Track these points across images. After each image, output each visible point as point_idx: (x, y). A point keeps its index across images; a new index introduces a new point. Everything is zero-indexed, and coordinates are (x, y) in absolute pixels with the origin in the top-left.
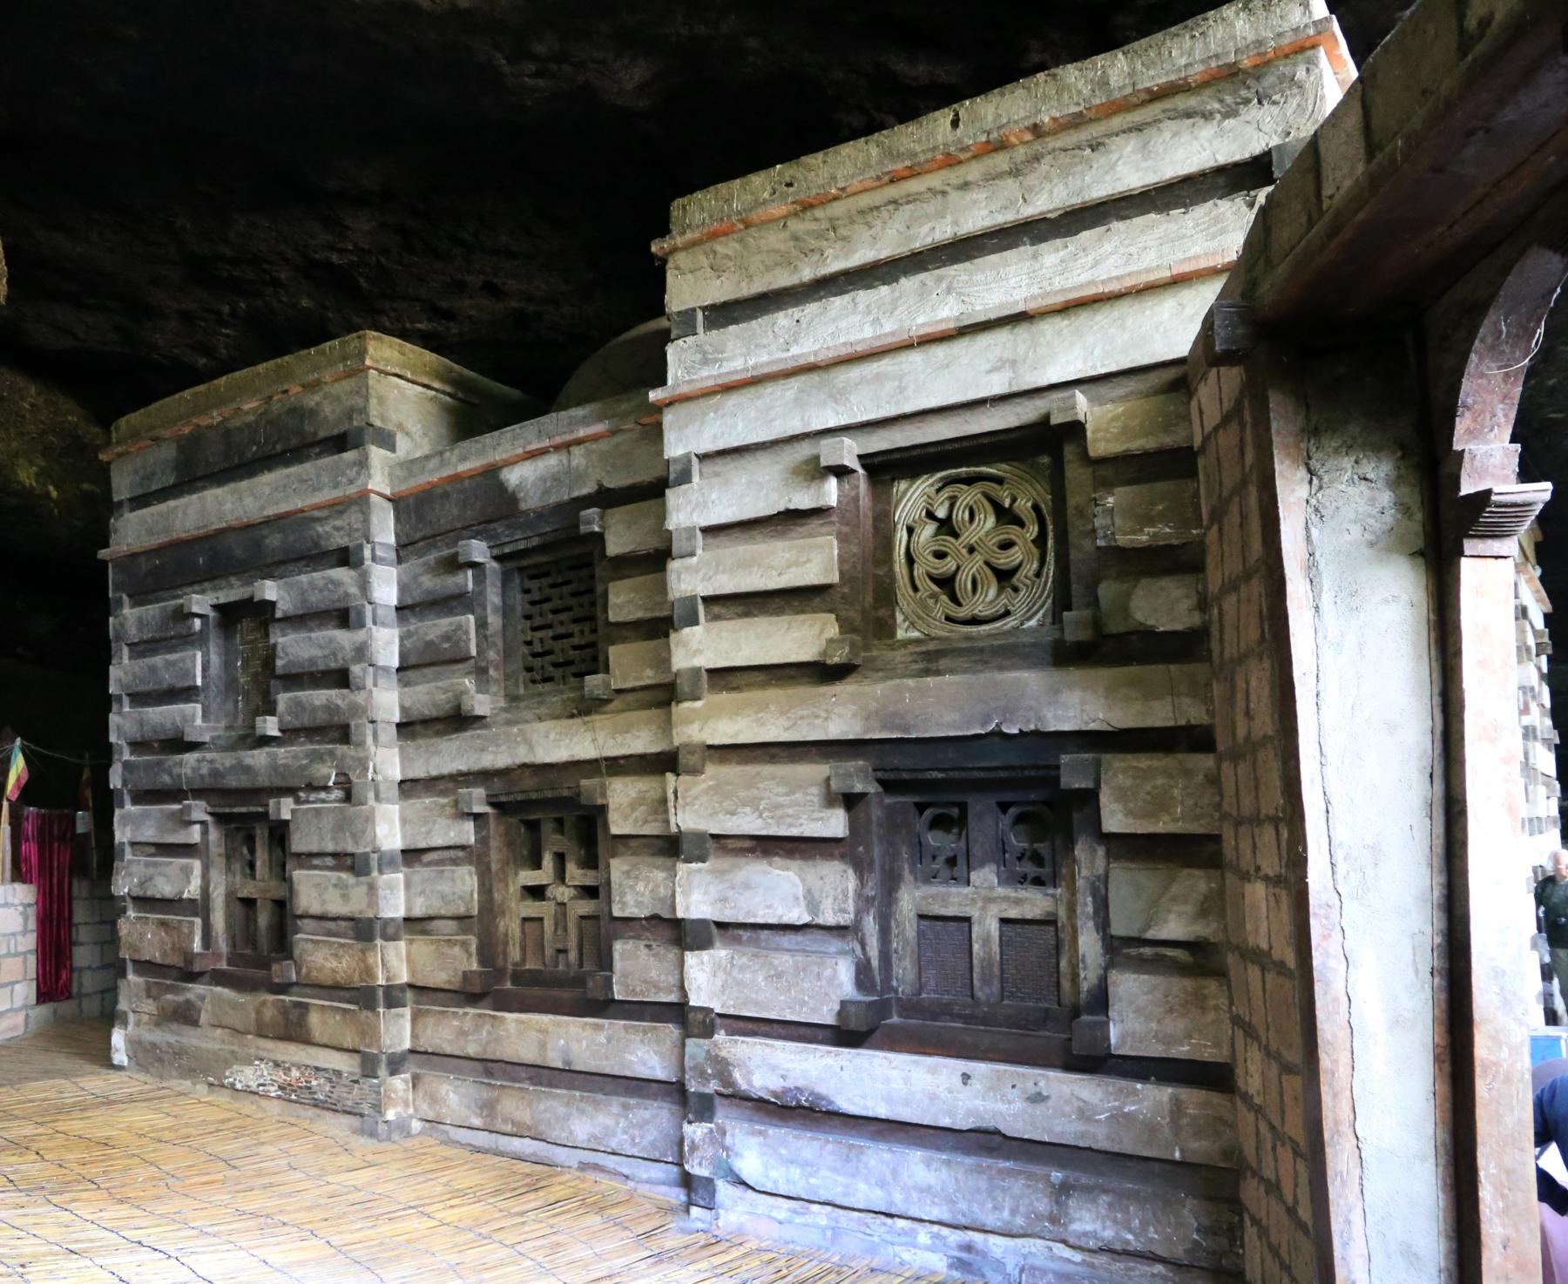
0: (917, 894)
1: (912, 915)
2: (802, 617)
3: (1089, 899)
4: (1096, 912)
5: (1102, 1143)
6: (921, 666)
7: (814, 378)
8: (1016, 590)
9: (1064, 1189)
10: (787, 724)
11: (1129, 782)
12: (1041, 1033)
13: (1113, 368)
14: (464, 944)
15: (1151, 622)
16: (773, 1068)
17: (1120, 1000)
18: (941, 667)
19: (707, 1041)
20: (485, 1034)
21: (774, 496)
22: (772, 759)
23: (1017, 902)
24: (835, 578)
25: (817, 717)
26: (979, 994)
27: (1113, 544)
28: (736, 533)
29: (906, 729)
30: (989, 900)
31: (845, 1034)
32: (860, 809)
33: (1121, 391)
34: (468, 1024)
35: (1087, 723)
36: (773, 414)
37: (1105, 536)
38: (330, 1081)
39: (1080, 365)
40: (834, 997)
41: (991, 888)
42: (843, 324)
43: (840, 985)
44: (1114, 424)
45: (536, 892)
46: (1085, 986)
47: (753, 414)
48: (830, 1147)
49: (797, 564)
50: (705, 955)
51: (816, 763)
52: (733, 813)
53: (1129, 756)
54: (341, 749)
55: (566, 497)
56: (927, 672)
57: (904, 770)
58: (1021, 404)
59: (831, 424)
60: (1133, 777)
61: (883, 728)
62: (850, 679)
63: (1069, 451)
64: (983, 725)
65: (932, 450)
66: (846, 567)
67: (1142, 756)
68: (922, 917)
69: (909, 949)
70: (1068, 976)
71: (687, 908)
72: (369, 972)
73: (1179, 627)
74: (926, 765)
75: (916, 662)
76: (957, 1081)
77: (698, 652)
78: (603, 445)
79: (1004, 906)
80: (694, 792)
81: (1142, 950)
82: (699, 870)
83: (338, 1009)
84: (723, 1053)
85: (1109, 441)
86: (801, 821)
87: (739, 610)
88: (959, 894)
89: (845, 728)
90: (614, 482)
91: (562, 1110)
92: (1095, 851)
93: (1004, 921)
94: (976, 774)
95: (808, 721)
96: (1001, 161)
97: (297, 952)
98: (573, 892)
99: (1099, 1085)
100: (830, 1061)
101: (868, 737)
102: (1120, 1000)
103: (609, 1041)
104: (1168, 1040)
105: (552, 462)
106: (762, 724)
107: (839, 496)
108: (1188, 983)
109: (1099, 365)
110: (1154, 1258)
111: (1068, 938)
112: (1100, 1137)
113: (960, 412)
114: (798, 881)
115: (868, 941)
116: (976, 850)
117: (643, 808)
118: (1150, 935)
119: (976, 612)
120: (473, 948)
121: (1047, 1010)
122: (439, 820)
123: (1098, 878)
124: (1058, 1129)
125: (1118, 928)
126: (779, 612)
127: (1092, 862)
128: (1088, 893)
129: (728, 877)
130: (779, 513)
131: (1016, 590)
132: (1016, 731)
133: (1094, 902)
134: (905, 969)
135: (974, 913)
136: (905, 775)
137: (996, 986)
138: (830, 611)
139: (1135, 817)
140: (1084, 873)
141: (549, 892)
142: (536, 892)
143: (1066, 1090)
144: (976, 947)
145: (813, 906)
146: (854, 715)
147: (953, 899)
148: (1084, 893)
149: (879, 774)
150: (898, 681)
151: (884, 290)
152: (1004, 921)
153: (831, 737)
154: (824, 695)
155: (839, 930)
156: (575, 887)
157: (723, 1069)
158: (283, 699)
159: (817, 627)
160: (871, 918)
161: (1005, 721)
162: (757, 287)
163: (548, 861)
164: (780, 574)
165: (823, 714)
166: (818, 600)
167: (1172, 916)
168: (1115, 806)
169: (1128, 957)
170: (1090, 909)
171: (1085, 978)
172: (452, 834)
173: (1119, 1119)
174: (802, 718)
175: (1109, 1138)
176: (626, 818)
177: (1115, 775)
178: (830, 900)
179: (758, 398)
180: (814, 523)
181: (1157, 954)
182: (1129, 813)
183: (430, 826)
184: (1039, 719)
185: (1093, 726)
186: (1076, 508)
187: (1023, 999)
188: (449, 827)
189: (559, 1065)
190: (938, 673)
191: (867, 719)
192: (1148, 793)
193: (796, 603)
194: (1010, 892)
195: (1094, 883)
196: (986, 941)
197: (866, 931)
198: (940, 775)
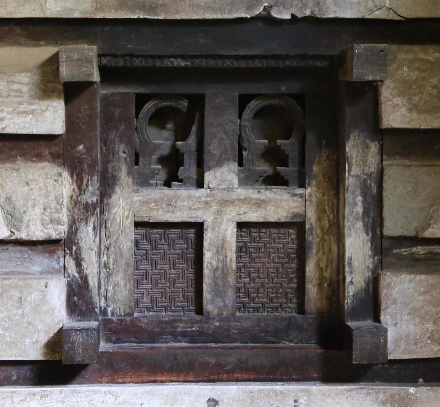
1: (129, 223)
3: (360, 198)
4: (366, 212)
11: (414, 75)
12: (281, 345)
17: (394, 302)
23: (259, 204)
29: (152, 9)
30: (224, 203)
35: (372, 11)
40: (40, 327)
41: (230, 190)
43: (51, 312)
51: (20, 44)
53: (416, 48)
57: (137, 56)
60: (418, 69)
61: (121, 6)
64: (249, 8)
67: (430, 49)
68: (138, 225)
69: (122, 262)
70: (315, 282)
74: (169, 51)
79: (244, 209)
81: (414, 249)
88: (189, 197)
92: (368, 147)
93: (241, 225)
94: (228, 63)
99: (368, 394)
101: (100, 16)
102: (394, 302)
111: (317, 240)
115: (85, 255)
118: (428, 234)
121: (290, 318)
123: (370, 175)
127: (364, 161)
128: (358, 192)
132: (288, 17)
133: (364, 201)
134: (116, 285)
136: (137, 62)
137: (231, 295)
139: (419, 112)
140: (355, 170)
144: (208, 256)
148: (354, 192)
149: (105, 61)
152: (241, 225)
153: (48, 15)
160: (91, 229)
161: (276, 4)
168: (398, 100)
169: (399, 257)
170: (360, 209)
171: (351, 282)
177: (399, 67)
178: (38, 210)
181: (431, 253)
185: (377, 14)
187: (257, 309)
192: (435, 87)
197: (83, 245)
198: (183, 64)
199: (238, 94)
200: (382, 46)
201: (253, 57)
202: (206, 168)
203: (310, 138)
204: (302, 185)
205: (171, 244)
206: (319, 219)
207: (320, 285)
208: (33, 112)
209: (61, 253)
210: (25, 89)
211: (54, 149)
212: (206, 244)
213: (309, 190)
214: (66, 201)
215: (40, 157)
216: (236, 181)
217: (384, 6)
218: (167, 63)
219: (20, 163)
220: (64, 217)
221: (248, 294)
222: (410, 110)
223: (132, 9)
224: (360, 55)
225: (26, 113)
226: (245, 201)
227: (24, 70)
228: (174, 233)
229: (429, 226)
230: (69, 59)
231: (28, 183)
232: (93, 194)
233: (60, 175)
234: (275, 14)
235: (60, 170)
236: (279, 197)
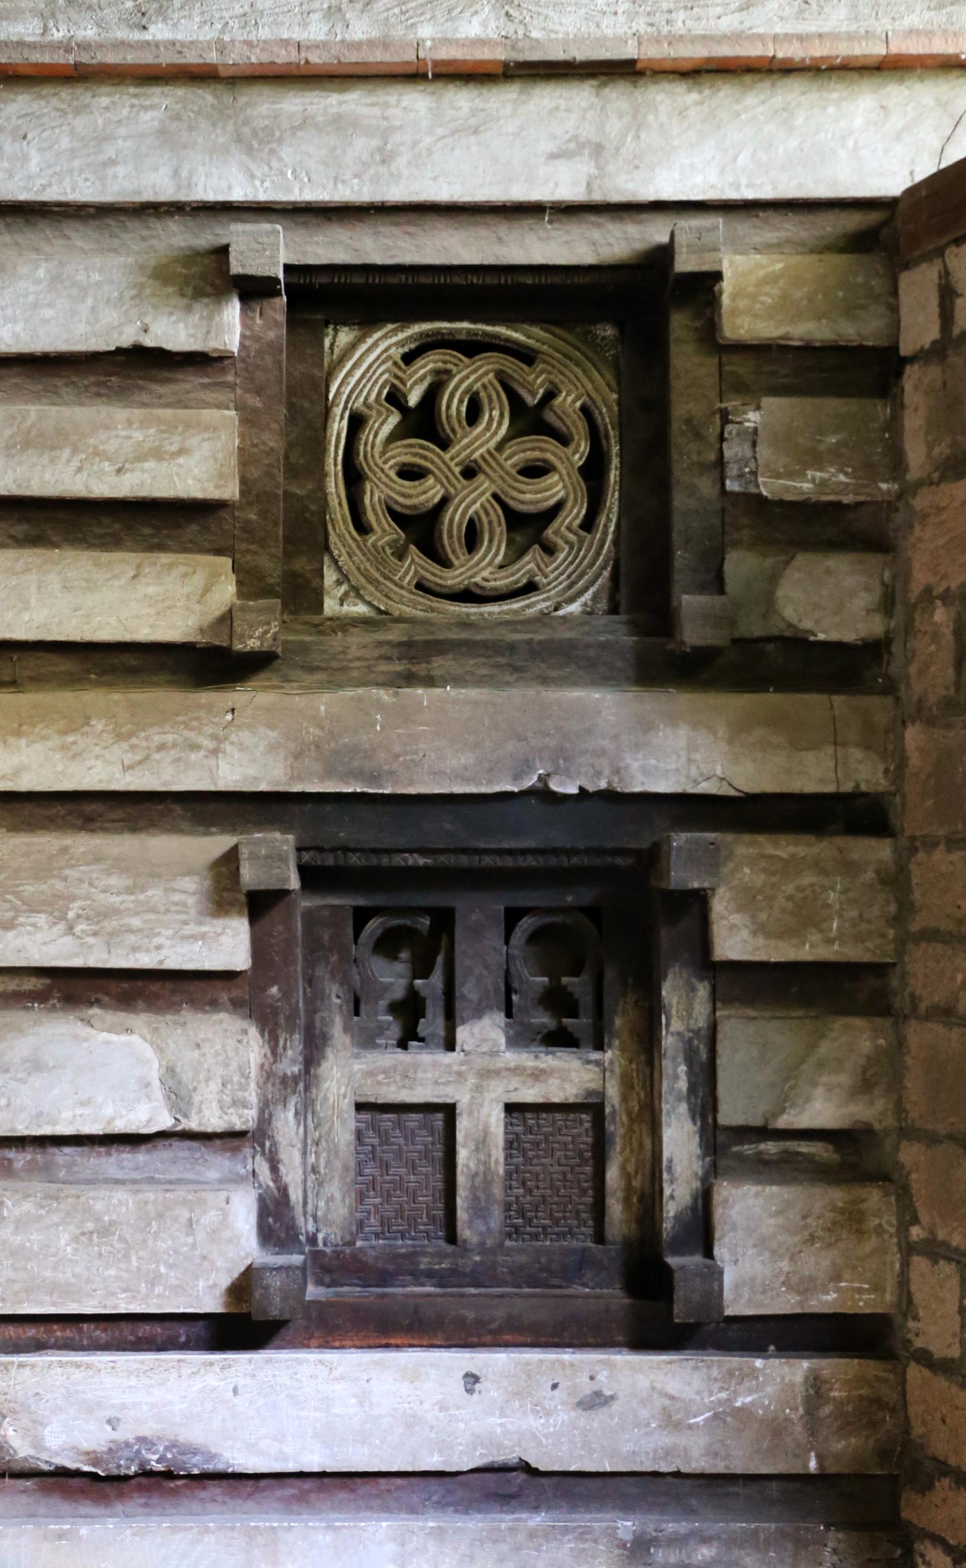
0: (357, 1066)
1: (347, 1105)
2: (165, 558)
5: (698, 1463)
6: (398, 667)
7: (205, 97)
8: (550, 550)
10: (128, 758)
11: (760, 880)
12: (570, 1291)
13: (766, 193)
15: (807, 624)
16: (90, 1409)
18: (436, 673)
21: (110, 316)
22: (88, 824)
23: (538, 1075)
24: (230, 491)
25: (195, 747)
26: (465, 1232)
27: (753, 490)
29: (374, 778)
30: (487, 1074)
32: (274, 920)
33: (770, 236)
35: (696, 783)
36: (110, 151)
37: (741, 476)
39: (713, 178)
41: (494, 1054)
44: (767, 289)
46: (671, 1210)
47: (65, 142)
49: (157, 454)
51: (181, 832)
53: (761, 838)
56: (410, 679)
57: (354, 850)
58: (599, 226)
59: (238, 194)
60: (764, 870)
61: (329, 773)
62: (257, 681)
64: (517, 777)
65: (426, 280)
66: (255, 473)
67: (783, 839)
68: (361, 1107)
69: (338, 1165)
70: (620, 1194)
73: (849, 636)
74: (402, 842)
75: (388, 658)
76: (456, 1385)
79: (515, 1082)
85: (756, 316)
86: (157, 941)
87: (20, 529)
88: (435, 1065)
89: (252, 771)
92: (693, 989)
93: (511, 1109)
94: (487, 860)
95: (174, 753)
100: (211, 1379)
101: (297, 788)
104: (805, 1287)
107: (243, 336)
108: (838, 1195)
109: (744, 181)
111: (622, 1131)
112: (696, 1452)
113: (489, 218)
116: (467, 990)
119: (478, 579)
121: (584, 1250)
123: (697, 1032)
124: (626, 1448)
126: (112, 542)
127: (689, 1009)
130: (119, 351)
131: (550, 550)
132: (573, 790)
135: (461, 1096)
136: (355, 860)
138: (219, 552)
139: (768, 936)
140: (677, 1025)
143: (643, 1382)
144: (462, 1155)
146: (272, 748)
149: (306, 857)
150: (360, 691)
152: (511, 1109)
153: (222, 786)
154: (209, 708)
159: (198, 580)
161: (556, 772)
164: (119, 471)
165: (208, 744)
166: (194, 528)
167: (819, 1091)
174: (161, 748)
175: (712, 1453)
177: (738, 869)
179: (78, 111)
180: (190, 382)
182: (759, 929)
184: (617, 771)
185: (705, 787)
186: (689, 421)
187: (535, 1237)
190: (430, 681)
191: (297, 756)
192: (790, 898)
193: (147, 531)
194: (525, 1059)
195: (690, 1040)
196: (482, 1142)
198: (422, 861)
199: (502, 908)
200: (711, 836)
201: (524, 852)
202: (458, 1020)
203: (610, 975)
204: (599, 1046)
205: (410, 1136)
206: (624, 1099)
207: (627, 1200)
208: (203, 937)
209: (248, 1151)
210: (191, 901)
211: (236, 993)
212: (460, 1137)
213: (609, 1054)
214: (254, 1072)
216: (503, 1040)
217: (715, 775)
218: (398, 860)
219: (187, 1014)
220: (252, 1095)
221: (522, 1213)
222: (754, 933)
223: (345, 777)
224: (679, 848)
225: (194, 937)
226: (517, 1071)
227: (189, 872)
228: (413, 1120)
229: (783, 1111)
230: (254, 857)
231: (198, 1046)
232: (294, 1061)
233: (245, 1032)
234: (556, 786)
235: (245, 1024)
236: (566, 1066)
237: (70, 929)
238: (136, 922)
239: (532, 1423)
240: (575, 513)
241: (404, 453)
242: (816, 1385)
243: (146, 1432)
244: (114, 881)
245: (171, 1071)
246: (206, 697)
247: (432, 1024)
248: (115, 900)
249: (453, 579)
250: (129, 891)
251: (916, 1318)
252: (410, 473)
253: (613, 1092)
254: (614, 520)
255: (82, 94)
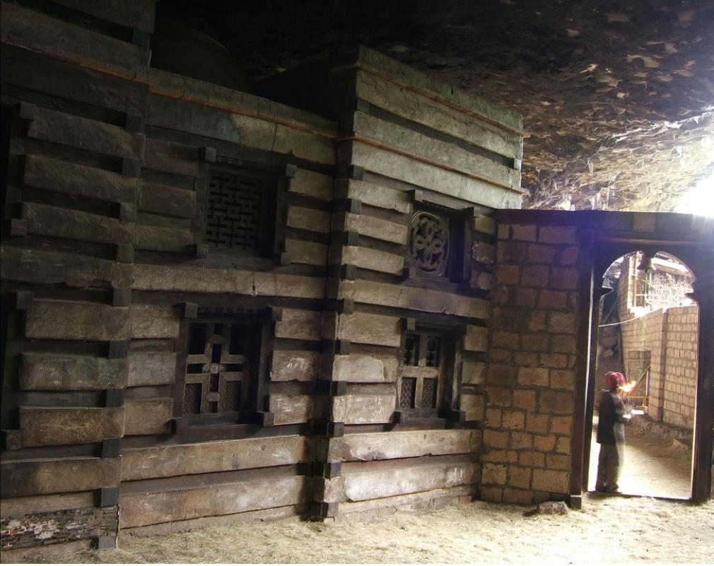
7: (408, 160)
9: (446, 470)
14: (165, 403)
19: (340, 438)
20: (177, 460)
21: (390, 202)
23: (429, 372)
26: (416, 406)
28: (371, 210)
31: (394, 423)
34: (164, 455)
38: (57, 520)
42: (417, 144)
45: (197, 369)
48: (383, 474)
50: (343, 398)
52: (362, 333)
54: (103, 262)
55: (269, 149)
63: (467, 223)
71: (337, 377)
72: (115, 429)
77: (355, 258)
78: (296, 132)
80: (347, 322)
82: (345, 359)
83: (75, 462)
84: (347, 442)
90: (299, 154)
91: (232, 494)
96: (463, 117)
97: (24, 422)
98: (221, 367)
103: (263, 449)
105: (266, 125)
106: (377, 296)
110: (459, 486)
114: (382, 364)
116: (421, 354)
117: (296, 325)
120: (172, 406)
122: (156, 320)
125: (462, 382)
129: (356, 362)
135: (418, 377)
138: (401, 255)
141: (204, 369)
142: (197, 369)
145: (386, 375)
147: (412, 371)
151: (430, 139)
155: (392, 383)
156: (223, 364)
157: (346, 448)
158: (31, 210)
162: (392, 109)
163: (209, 349)
172: (166, 330)
173: (460, 442)
174: (390, 296)
175: (457, 450)
176: (286, 329)
183: (149, 323)
185: (466, 315)
188: (164, 326)
189: (230, 468)
215: (391, 354)
237: (372, 336)
238: (383, 334)
239: (432, 445)
240: (442, 255)
241: (419, 238)
242: (471, 435)
243: (375, 450)
244: (380, 325)
245: (385, 368)
246: (397, 286)
247: (413, 360)
248: (380, 329)
249: (424, 266)
250: (382, 328)
251: (487, 420)
252: (420, 242)
253: (439, 376)
254: (630, 278)
255: (391, 154)
